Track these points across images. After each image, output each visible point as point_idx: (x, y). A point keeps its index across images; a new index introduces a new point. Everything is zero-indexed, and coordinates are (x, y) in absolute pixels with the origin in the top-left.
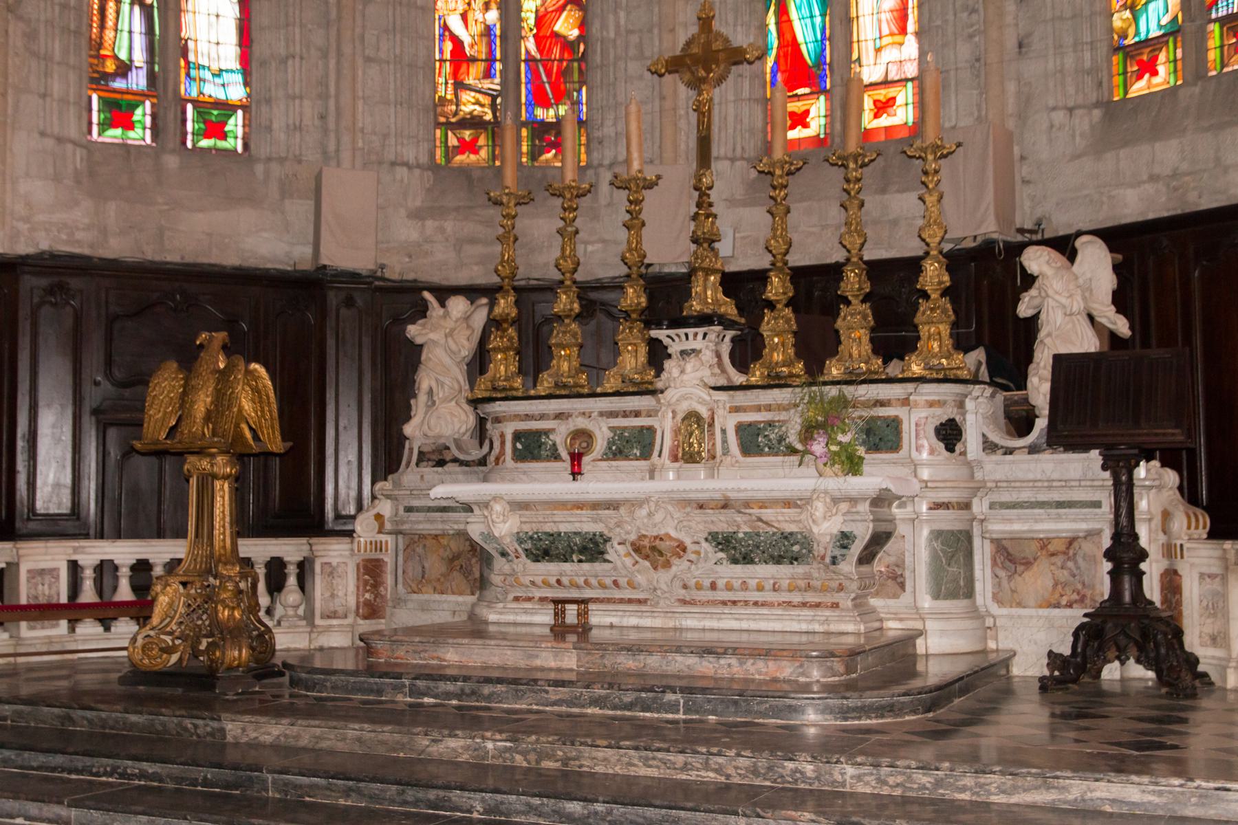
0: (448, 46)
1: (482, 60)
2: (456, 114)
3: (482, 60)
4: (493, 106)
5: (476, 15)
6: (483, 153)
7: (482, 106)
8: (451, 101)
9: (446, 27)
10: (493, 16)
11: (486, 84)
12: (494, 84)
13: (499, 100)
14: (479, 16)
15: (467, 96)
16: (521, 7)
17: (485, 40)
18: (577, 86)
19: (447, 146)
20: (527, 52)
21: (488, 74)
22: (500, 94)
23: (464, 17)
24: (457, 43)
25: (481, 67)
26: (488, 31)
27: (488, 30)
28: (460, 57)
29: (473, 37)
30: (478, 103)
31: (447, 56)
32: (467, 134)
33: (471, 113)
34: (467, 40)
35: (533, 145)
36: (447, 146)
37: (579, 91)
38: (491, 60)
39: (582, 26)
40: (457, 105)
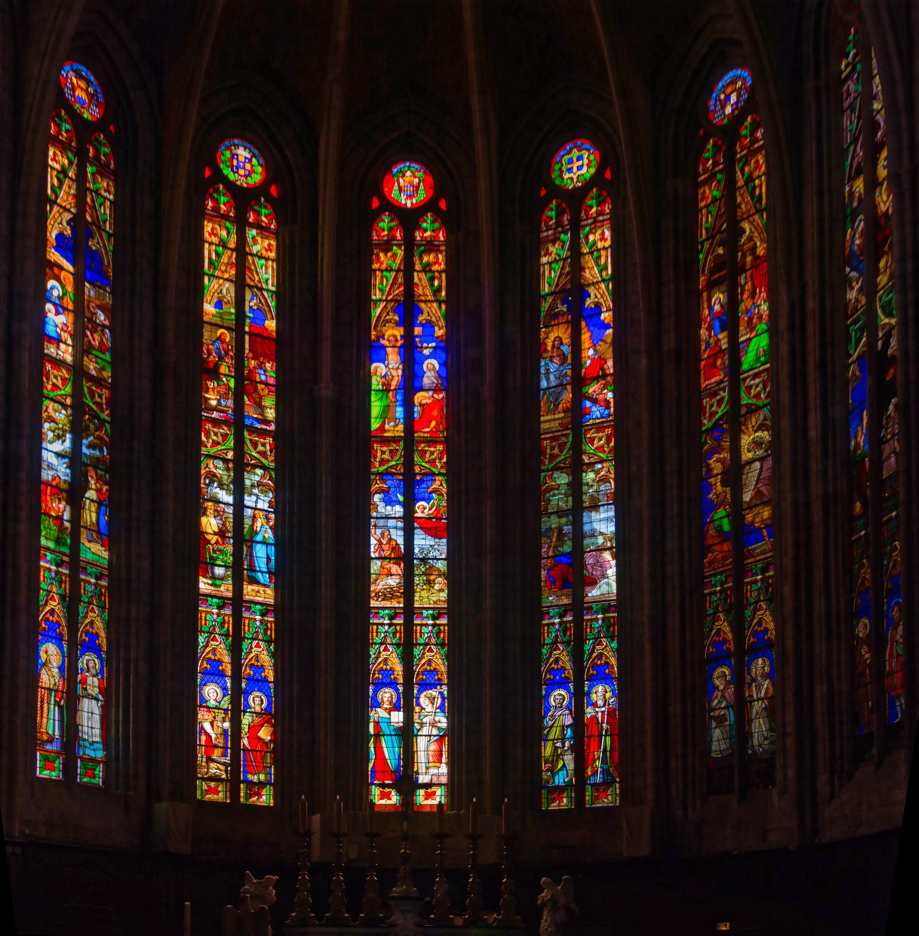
0: (203, 738)
1: (221, 747)
2: (207, 773)
3: (221, 747)
4: (226, 771)
5: (218, 723)
6: (221, 795)
7: (221, 770)
8: (204, 766)
9: (202, 728)
10: (227, 725)
11: (223, 760)
12: (227, 760)
13: (229, 768)
14: (220, 725)
15: (212, 765)
16: (241, 721)
17: (223, 736)
18: (269, 765)
19: (202, 790)
20: (244, 745)
21: (224, 755)
22: (230, 765)
23: (212, 723)
24: (208, 736)
25: (220, 750)
26: (225, 732)
27: (225, 732)
28: (210, 746)
29: (216, 734)
30: (218, 769)
31: (203, 743)
32: (212, 784)
33: (215, 773)
34: (213, 736)
35: (247, 793)
36: (202, 790)
37: (270, 768)
38: (225, 748)
39: (273, 734)
40: (208, 769)
